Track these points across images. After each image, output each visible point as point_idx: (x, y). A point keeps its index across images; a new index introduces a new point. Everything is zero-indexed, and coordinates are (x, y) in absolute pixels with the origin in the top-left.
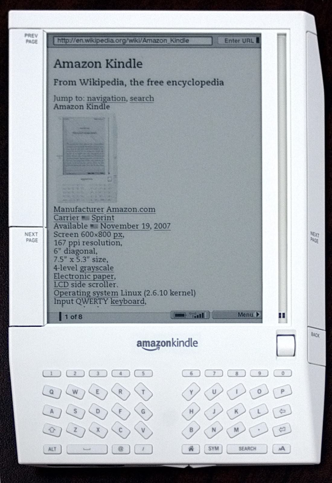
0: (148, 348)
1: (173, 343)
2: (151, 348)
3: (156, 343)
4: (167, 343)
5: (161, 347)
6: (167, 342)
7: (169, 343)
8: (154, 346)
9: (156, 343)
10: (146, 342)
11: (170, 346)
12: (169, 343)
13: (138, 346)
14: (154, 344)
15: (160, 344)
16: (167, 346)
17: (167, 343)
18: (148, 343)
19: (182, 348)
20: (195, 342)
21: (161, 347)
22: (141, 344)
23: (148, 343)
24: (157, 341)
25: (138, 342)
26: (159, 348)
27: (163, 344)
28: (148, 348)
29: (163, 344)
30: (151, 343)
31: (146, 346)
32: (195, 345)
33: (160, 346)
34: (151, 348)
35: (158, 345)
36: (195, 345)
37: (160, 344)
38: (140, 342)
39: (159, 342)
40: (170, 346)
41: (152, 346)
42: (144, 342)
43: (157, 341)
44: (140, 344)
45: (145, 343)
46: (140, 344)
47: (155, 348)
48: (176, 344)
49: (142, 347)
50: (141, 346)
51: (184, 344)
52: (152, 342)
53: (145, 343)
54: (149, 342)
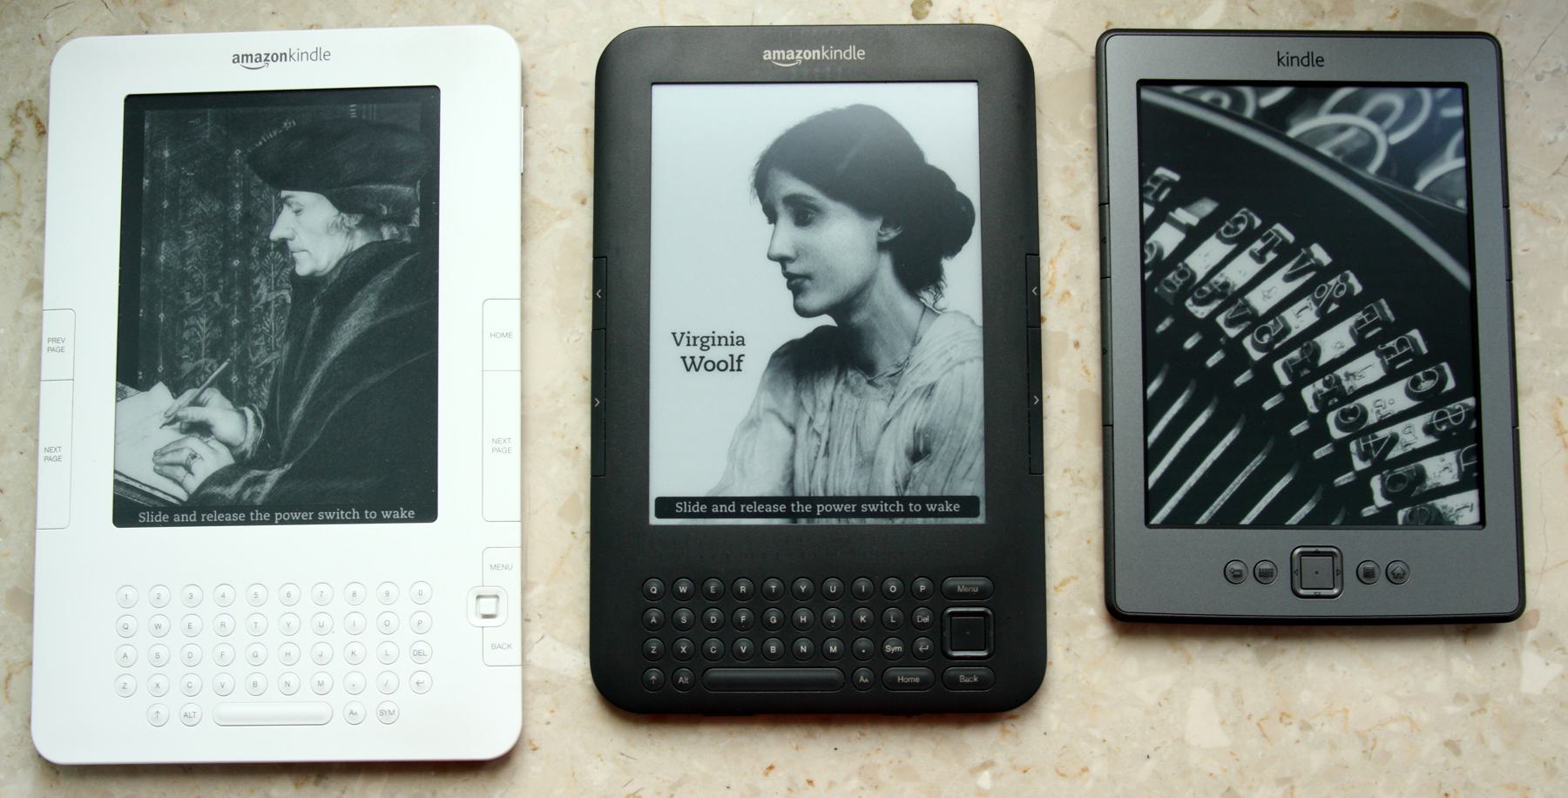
1: (291, 56)
3: (264, 57)
4: (282, 57)
5: (271, 63)
6: (281, 54)
7: (283, 56)
8: (260, 61)
9: (264, 57)
10: (247, 56)
11: (286, 60)
12: (283, 56)
14: (260, 57)
15: (269, 58)
16: (281, 60)
17: (282, 57)
18: (250, 57)
19: (305, 63)
20: (327, 54)
21: (271, 63)
22: (238, 58)
23: (250, 57)
27: (275, 59)
28: (250, 65)
29: (275, 57)
31: (247, 61)
32: (326, 57)
34: (254, 65)
35: (266, 60)
36: (326, 57)
37: (269, 58)
38: (238, 56)
39: (268, 55)
40: (286, 60)
41: (256, 61)
44: (237, 59)
45: (245, 57)
46: (237, 59)
47: (260, 64)
48: (295, 57)
50: (238, 61)
51: (309, 57)
53: (245, 57)
54: (251, 55)
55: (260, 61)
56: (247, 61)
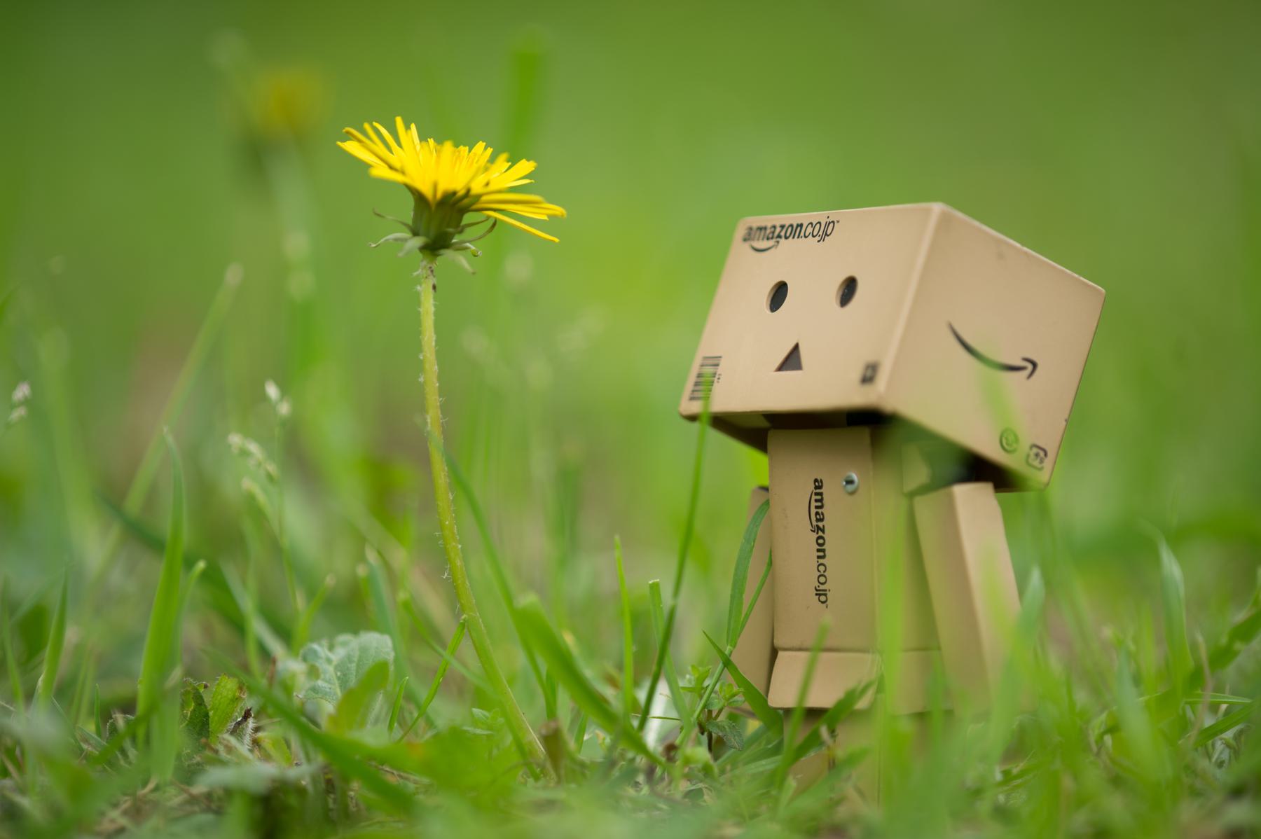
0: (814, 504)
2: (813, 511)
3: (820, 524)
5: (815, 536)
8: (818, 520)
9: (820, 524)
10: (821, 500)
11: (819, 557)
12: (821, 554)
13: (816, 480)
18: (819, 504)
21: (815, 536)
23: (819, 504)
24: (824, 526)
25: (821, 480)
26: (814, 531)
28: (814, 504)
29: (821, 541)
30: (820, 511)
31: (816, 501)
33: (817, 533)
34: (813, 511)
39: (823, 531)
41: (817, 513)
42: (821, 494)
43: (824, 526)
47: (814, 523)
49: (815, 491)
50: (816, 488)
52: (823, 514)
55: (818, 520)
56: (816, 501)
